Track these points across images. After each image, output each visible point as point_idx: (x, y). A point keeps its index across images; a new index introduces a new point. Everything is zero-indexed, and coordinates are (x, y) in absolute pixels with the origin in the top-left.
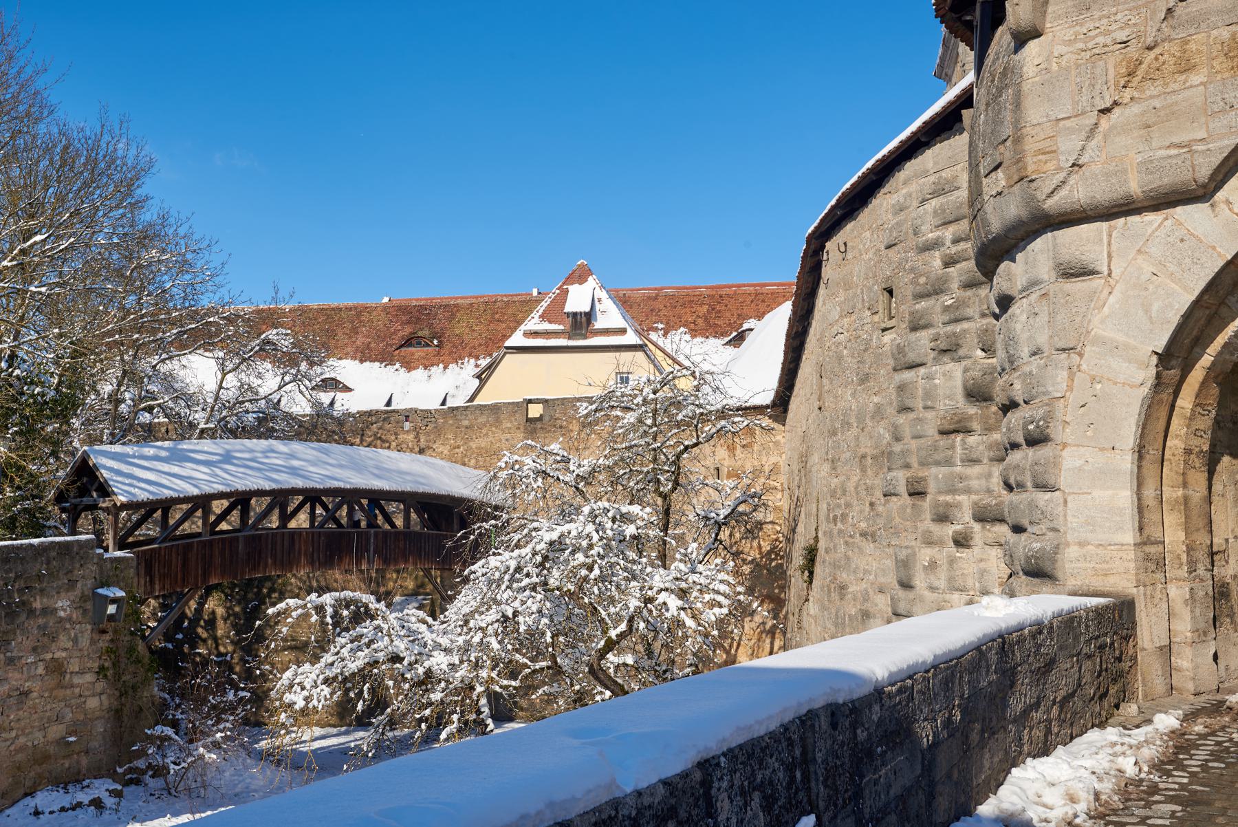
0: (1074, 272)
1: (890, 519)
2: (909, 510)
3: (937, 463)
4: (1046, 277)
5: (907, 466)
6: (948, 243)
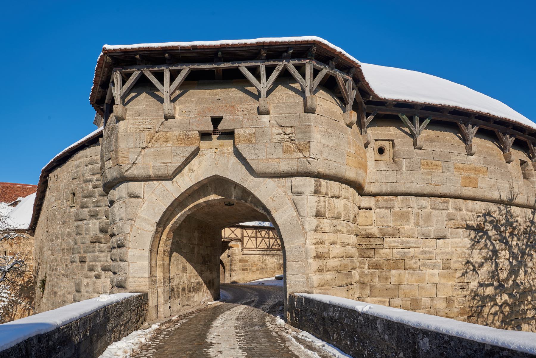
0: (134, 196)
1: (73, 270)
2: (80, 267)
3: (90, 252)
4: (125, 196)
5: (79, 253)
6: (95, 181)
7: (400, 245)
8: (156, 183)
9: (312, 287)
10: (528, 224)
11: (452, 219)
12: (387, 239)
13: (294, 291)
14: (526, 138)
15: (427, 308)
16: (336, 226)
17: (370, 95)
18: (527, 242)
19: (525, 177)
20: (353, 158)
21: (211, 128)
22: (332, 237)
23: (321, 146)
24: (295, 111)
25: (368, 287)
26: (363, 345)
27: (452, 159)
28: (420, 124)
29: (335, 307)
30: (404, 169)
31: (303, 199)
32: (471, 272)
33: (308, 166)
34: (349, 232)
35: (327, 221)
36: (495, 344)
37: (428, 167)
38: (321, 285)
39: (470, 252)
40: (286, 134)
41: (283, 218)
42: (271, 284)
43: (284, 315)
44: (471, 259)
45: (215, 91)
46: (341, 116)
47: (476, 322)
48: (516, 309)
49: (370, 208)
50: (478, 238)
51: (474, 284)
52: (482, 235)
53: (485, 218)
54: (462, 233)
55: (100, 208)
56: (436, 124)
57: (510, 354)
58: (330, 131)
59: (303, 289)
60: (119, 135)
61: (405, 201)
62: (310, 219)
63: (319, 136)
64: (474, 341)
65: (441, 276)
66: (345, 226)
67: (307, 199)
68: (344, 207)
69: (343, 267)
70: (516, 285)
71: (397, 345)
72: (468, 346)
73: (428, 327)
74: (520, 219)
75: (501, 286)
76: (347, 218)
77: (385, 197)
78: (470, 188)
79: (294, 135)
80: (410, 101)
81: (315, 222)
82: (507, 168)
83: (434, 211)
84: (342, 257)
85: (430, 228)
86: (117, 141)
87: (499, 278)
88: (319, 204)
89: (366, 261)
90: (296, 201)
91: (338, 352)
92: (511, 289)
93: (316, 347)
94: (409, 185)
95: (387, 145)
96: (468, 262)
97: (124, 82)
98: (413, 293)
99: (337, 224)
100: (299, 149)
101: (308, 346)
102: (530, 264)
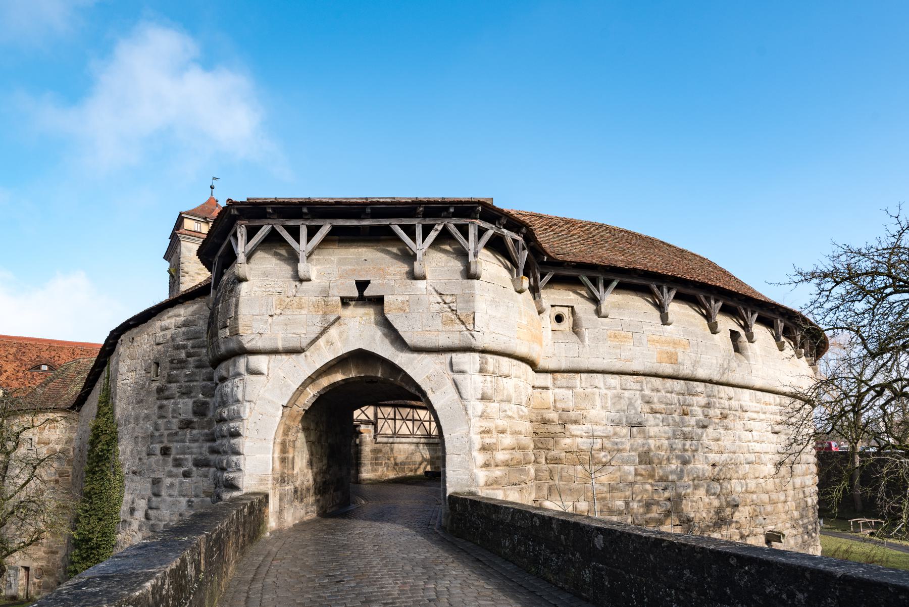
1: (150, 466)
5: (161, 442)
8: (284, 357)
21: (356, 294)
30: (587, 342)
35: (496, 405)
41: (442, 402)
45: (360, 250)
49: (547, 388)
55: (195, 383)
60: (241, 300)
63: (484, 306)
86: (237, 306)
89: (543, 454)
90: (458, 382)
95: (566, 312)
97: (249, 239)
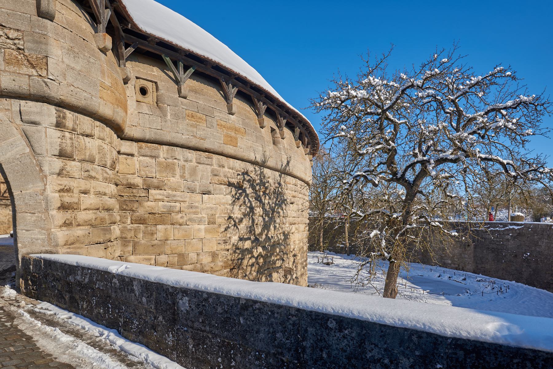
7: (165, 199)
9: (57, 245)
10: (277, 185)
11: (216, 175)
12: (152, 191)
13: (29, 251)
14: (275, 108)
15: (193, 264)
16: (88, 171)
17: (129, 22)
18: (276, 201)
19: (274, 143)
20: (109, 92)
22: (84, 185)
23: (64, 66)
24: (23, 10)
25: (131, 244)
26: (119, 312)
27: (215, 115)
28: (185, 72)
29: (83, 269)
30: (169, 117)
31: (39, 132)
32: (233, 227)
33: (46, 88)
34: (106, 180)
36: (248, 297)
37: (193, 119)
38: (69, 243)
39: (231, 207)
40: (8, 38)
42: (4, 243)
43: (16, 283)
44: (232, 215)
46: (91, 36)
47: (236, 276)
48: (268, 260)
49: (132, 155)
50: (238, 195)
51: (235, 239)
52: (241, 193)
53: (244, 177)
54: (225, 189)
56: (198, 75)
57: (261, 306)
58: (76, 50)
59: (44, 249)
61: (170, 151)
62: (50, 159)
64: (230, 297)
65: (207, 231)
66: (101, 171)
67: (46, 133)
68: (99, 149)
69: (98, 221)
70: (268, 239)
71: (156, 309)
72: (225, 302)
73: (188, 285)
74: (271, 181)
75: (257, 239)
76: (104, 162)
77: (149, 144)
78: (231, 147)
79: (22, 42)
80: (174, 43)
81: (58, 164)
82: (261, 132)
83: (199, 165)
84: (98, 209)
85: (196, 183)
87: (255, 232)
88: (64, 141)
91: (88, 323)
92: (265, 243)
93: (60, 320)
94: (174, 135)
95: (150, 87)
96: (230, 218)
98: (180, 249)
99: (89, 169)
100: (31, 64)
101: (47, 320)
102: (278, 221)
